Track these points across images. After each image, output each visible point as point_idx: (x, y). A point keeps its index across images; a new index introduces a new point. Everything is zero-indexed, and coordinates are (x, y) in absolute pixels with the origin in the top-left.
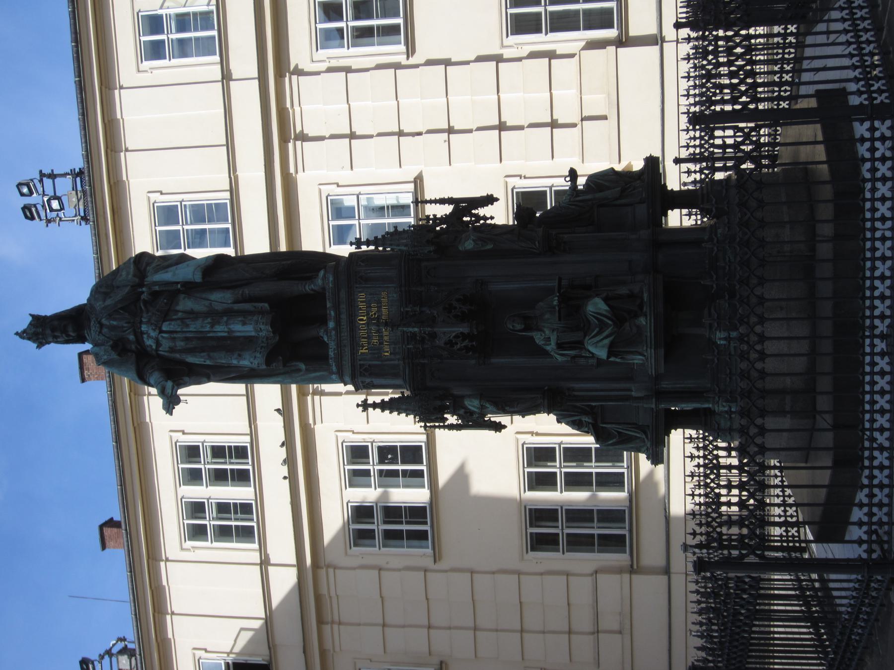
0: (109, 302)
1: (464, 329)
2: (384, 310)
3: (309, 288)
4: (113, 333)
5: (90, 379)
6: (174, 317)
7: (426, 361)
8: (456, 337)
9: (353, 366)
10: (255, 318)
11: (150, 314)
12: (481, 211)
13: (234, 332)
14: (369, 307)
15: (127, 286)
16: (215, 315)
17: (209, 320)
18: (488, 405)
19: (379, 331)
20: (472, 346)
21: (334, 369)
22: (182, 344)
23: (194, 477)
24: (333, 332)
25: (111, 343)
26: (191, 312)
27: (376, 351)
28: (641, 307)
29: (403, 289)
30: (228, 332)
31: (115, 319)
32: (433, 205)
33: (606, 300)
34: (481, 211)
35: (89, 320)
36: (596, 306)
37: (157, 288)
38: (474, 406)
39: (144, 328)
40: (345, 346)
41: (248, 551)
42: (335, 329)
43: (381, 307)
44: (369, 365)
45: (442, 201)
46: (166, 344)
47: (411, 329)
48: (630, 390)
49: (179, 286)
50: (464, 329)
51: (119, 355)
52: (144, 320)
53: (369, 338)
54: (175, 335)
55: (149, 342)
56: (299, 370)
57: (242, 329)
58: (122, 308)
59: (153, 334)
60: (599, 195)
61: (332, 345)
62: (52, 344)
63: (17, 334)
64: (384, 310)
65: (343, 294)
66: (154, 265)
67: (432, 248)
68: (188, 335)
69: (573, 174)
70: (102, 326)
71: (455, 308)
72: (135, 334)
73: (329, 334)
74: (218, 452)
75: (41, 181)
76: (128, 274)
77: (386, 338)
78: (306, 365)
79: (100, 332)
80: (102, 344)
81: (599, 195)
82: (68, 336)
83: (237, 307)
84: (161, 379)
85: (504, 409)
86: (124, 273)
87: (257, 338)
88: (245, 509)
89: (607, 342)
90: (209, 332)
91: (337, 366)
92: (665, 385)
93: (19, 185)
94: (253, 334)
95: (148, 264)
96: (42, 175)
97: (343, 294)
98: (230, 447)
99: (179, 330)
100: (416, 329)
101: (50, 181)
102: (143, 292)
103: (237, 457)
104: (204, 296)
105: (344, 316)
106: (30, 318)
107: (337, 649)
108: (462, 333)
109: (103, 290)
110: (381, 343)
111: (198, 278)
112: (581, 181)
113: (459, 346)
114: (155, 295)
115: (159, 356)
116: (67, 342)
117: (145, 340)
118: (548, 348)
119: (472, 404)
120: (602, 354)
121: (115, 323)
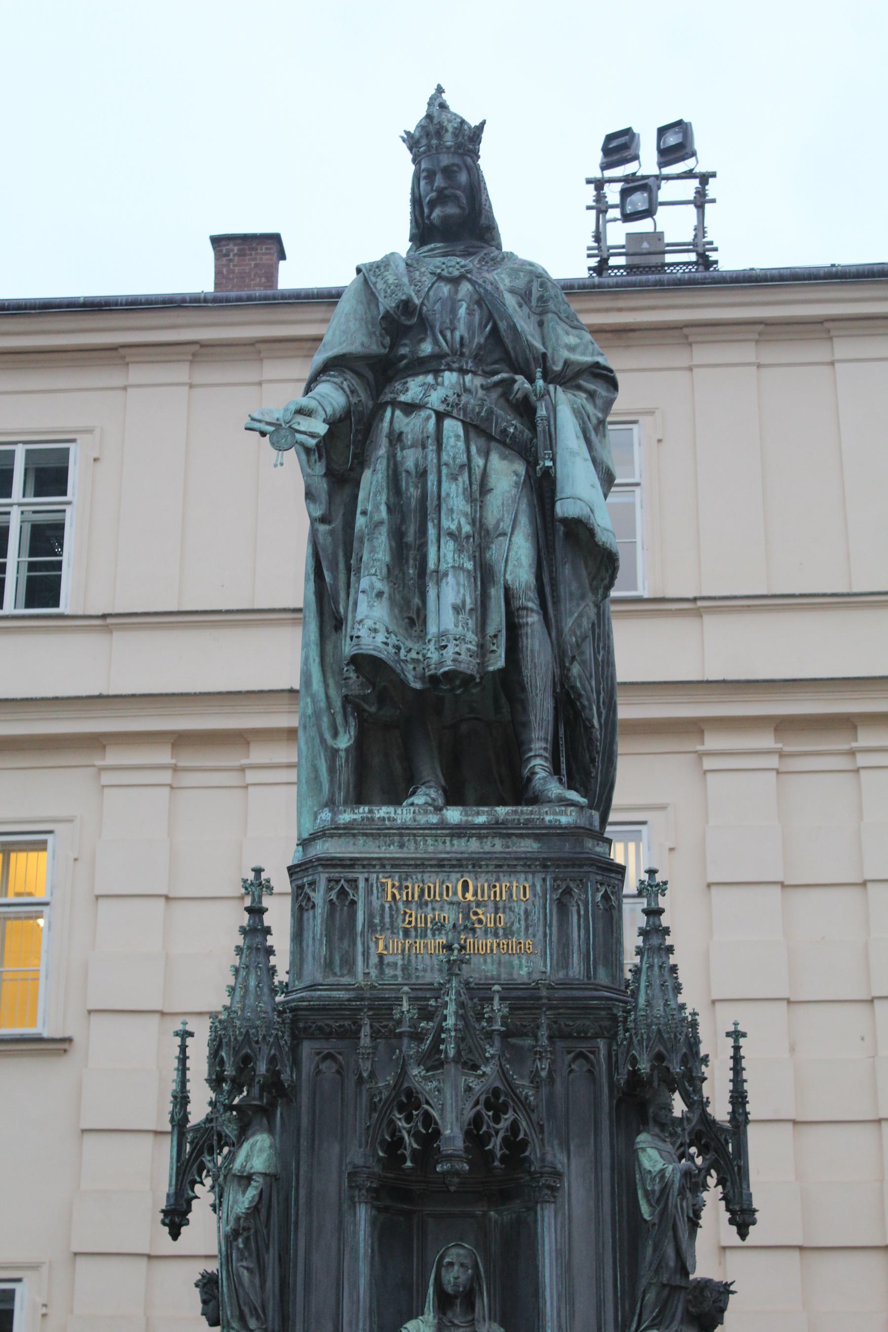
0: (510, 301)
1: (452, 1133)
3: (539, 766)
4: (438, 307)
5: (219, 255)
6: (473, 449)
7: (365, 1040)
8: (428, 1119)
9: (353, 863)
10: (471, 636)
11: (481, 393)
12: (712, 1197)
13: (438, 583)
15: (544, 344)
17: (467, 528)
19: (439, 928)
20: (403, 1159)
21: (346, 817)
22: (410, 464)
24: (434, 819)
25: (417, 301)
26: (484, 489)
29: (544, 993)
30: (437, 572)
31: (470, 312)
32: (731, 1075)
34: (712, 1197)
35: (466, 254)
37: (542, 412)
38: (248, 1157)
39: (450, 378)
40: (402, 846)
42: (443, 825)
43: (496, 935)
44: (353, 903)
45: (739, 1098)
47: (451, 1010)
49: (549, 463)
50: (452, 1133)
51: (387, 316)
52: (468, 377)
53: (422, 904)
54: (431, 447)
55: (414, 388)
56: (335, 735)
58: (495, 329)
59: (435, 399)
61: (402, 815)
62: (412, 168)
63: (440, 90)
65: (528, 846)
66: (590, 408)
67: (644, 1066)
68: (432, 478)
70: (455, 281)
71: (497, 1119)
72: (438, 357)
73: (420, 807)
75: (689, 175)
76: (572, 349)
78: (347, 750)
79: (440, 277)
80: (411, 280)
82: (432, 204)
83: (497, 594)
84: (329, 410)
85: (242, 1236)
86: (572, 340)
87: (422, 636)
90: (439, 527)
93: (679, 124)
94: (432, 629)
95: (591, 395)
96: (704, 178)
97: (528, 846)
98: (58, 566)
99: (444, 457)
100: (450, 1022)
101: (691, 196)
102: (532, 381)
103: (30, 580)
104: (524, 520)
105: (474, 845)
106: (474, 122)
108: (437, 1133)
109: (536, 292)
111: (564, 509)
113: (402, 1124)
114: (525, 409)
115: (380, 408)
116: (417, 202)
117: (420, 379)
119: (257, 1153)
121: (462, 311)
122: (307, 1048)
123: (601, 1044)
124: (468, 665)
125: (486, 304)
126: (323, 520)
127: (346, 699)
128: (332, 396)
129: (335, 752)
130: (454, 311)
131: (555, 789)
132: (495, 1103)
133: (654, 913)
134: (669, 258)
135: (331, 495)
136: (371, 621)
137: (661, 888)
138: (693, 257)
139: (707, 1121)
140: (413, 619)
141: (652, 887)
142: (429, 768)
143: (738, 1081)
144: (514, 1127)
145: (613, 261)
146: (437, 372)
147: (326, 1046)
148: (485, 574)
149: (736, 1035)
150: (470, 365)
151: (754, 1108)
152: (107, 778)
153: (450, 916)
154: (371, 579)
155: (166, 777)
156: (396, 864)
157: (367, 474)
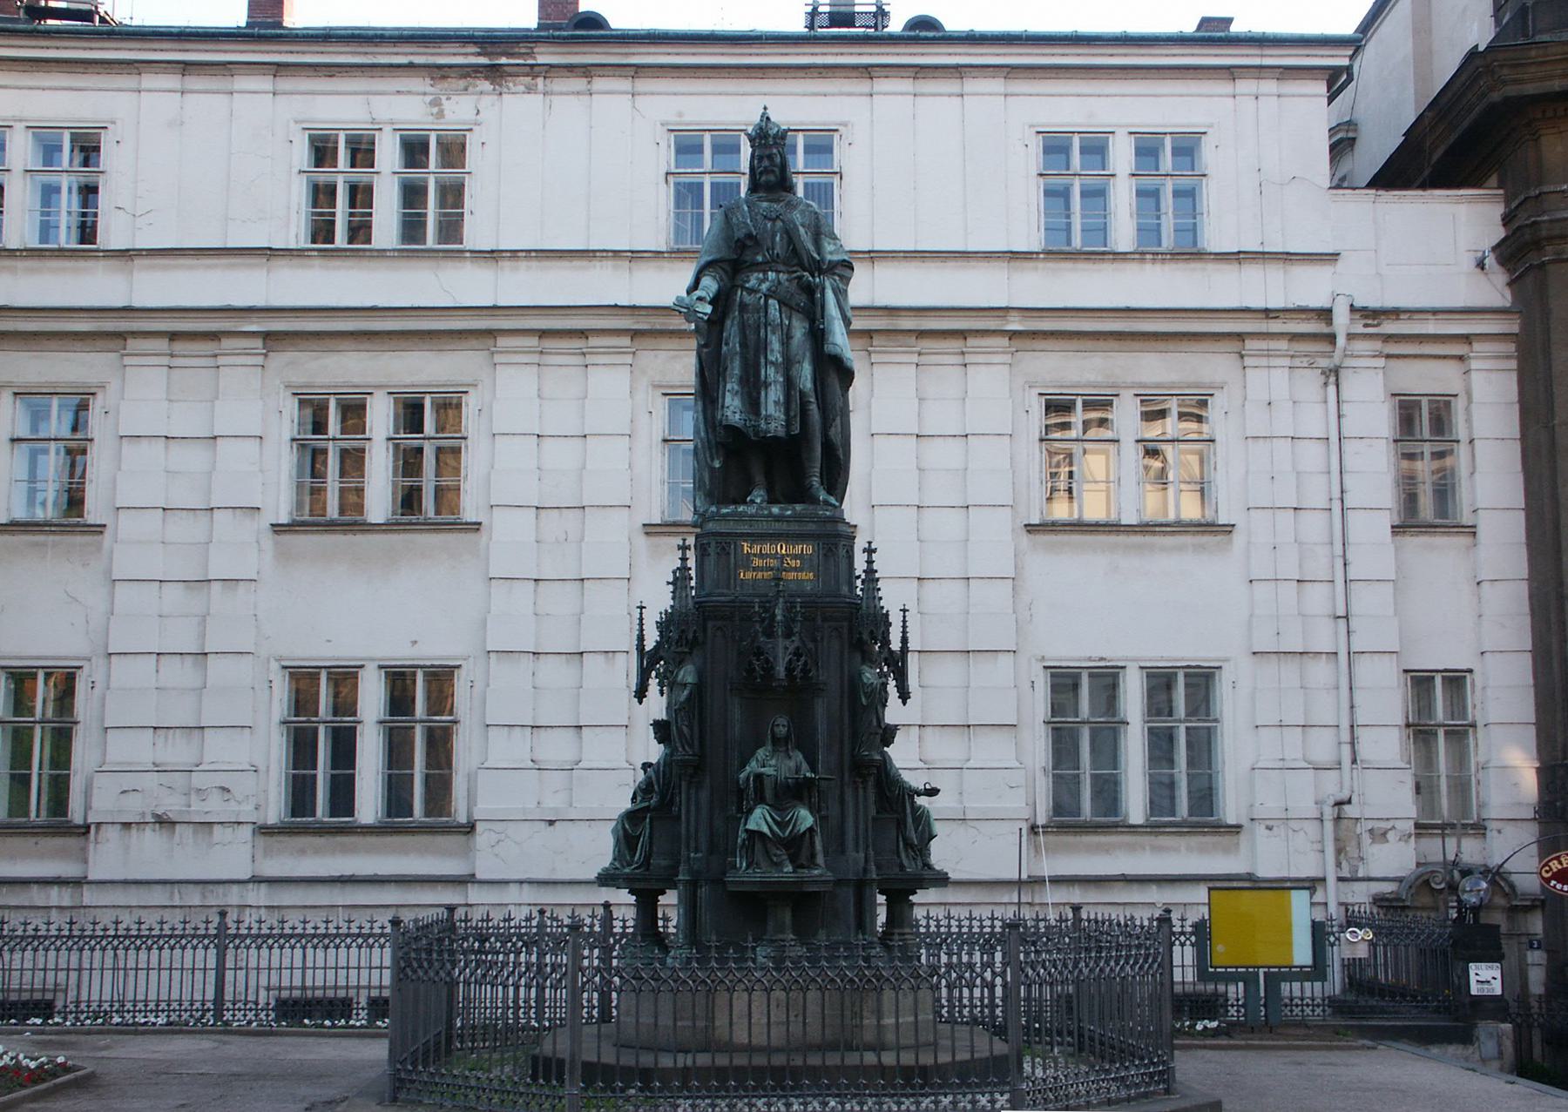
0: (802, 230)
1: (781, 670)
2: (791, 575)
8: (767, 661)
9: (729, 534)
12: (892, 684)
14: (795, 557)
16: (788, 365)
18: (686, 692)
21: (724, 511)
23: (414, 150)
27: (746, 562)
28: (802, 866)
33: (811, 829)
35: (778, 201)
36: (805, 818)
41: (296, 233)
42: (771, 515)
45: (904, 640)
46: (748, 299)
48: (696, 851)
50: (781, 670)
53: (761, 556)
57: (773, 396)
58: (794, 250)
59: (764, 287)
60: (910, 820)
61: (752, 510)
64: (791, 575)
65: (812, 527)
69: (933, 792)
72: (765, 263)
74: (453, 194)
77: (760, 575)
81: (910, 820)
87: (757, 413)
88: (360, 230)
89: (765, 829)
91: (727, 514)
92: (703, 892)
95: (841, 277)
105: (785, 526)
107: (127, 361)
108: (773, 668)
110: (754, 569)
112: (921, 801)
114: (809, 290)
115: (734, 287)
118: (754, 763)
119: (687, 674)
120: (751, 826)
122: (710, 624)
123: (845, 624)
124: (781, 432)
125: (790, 236)
126: (705, 346)
127: (717, 443)
128: (710, 285)
129: (712, 469)
130: (774, 236)
131: (822, 496)
132: (797, 654)
133: (870, 562)
134: (857, 9)
135: (709, 332)
136: (732, 407)
137: (874, 551)
138: (874, 9)
139: (891, 652)
140: (753, 403)
141: (870, 551)
142: (759, 478)
143: (904, 632)
144: (806, 663)
145: (821, 9)
146: (765, 272)
147: (719, 623)
148: (789, 384)
149: (904, 611)
150: (781, 267)
151: (911, 646)
152: (498, 358)
153: (773, 563)
154: (732, 385)
155: (535, 358)
156: (748, 535)
157: (728, 323)
